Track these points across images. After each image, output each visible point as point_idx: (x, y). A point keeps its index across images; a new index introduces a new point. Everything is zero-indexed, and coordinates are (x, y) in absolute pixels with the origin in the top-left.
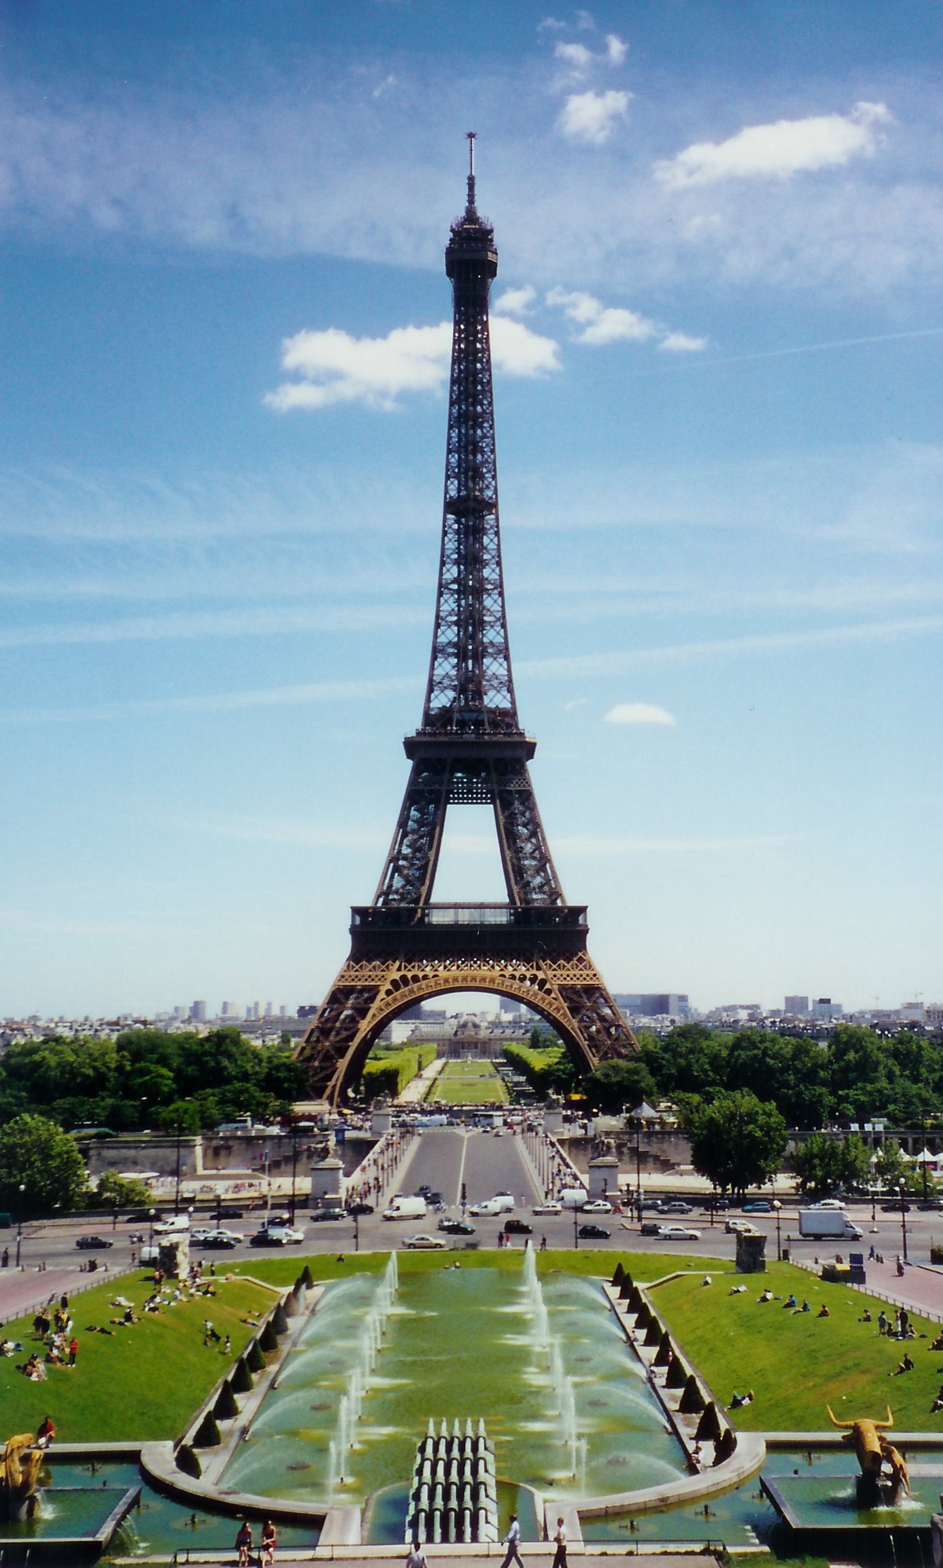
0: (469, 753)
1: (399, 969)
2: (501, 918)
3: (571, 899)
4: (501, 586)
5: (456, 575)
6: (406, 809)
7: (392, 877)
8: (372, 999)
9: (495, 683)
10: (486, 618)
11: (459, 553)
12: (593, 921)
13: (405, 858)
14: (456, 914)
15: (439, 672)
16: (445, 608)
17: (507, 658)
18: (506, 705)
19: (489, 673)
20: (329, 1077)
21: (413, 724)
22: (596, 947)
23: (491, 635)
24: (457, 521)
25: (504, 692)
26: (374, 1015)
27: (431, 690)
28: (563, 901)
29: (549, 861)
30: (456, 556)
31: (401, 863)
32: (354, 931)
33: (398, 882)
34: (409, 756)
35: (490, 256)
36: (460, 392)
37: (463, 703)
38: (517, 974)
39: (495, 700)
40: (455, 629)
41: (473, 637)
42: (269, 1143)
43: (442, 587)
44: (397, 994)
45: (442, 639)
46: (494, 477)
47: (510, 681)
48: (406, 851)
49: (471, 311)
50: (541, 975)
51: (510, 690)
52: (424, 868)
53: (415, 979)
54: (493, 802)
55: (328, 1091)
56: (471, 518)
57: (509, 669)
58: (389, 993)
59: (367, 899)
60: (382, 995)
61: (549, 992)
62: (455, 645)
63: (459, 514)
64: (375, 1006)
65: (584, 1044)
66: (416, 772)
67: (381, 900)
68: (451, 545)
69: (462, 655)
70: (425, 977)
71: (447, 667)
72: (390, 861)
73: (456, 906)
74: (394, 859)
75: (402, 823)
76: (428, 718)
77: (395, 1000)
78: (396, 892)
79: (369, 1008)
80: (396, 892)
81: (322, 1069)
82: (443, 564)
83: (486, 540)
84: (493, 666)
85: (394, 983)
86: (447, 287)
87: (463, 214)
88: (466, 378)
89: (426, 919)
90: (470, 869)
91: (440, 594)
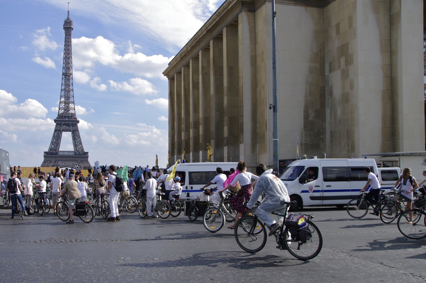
0: (66, 122)
2: (72, 154)
3: (86, 151)
6: (54, 133)
15: (61, 106)
16: (62, 94)
23: (71, 100)
32: (44, 156)
39: (71, 111)
43: (62, 90)
48: (54, 141)
52: (58, 144)
59: (47, 151)
63: (65, 76)
66: (56, 125)
69: (65, 103)
71: (63, 105)
74: (52, 142)
90: (67, 144)
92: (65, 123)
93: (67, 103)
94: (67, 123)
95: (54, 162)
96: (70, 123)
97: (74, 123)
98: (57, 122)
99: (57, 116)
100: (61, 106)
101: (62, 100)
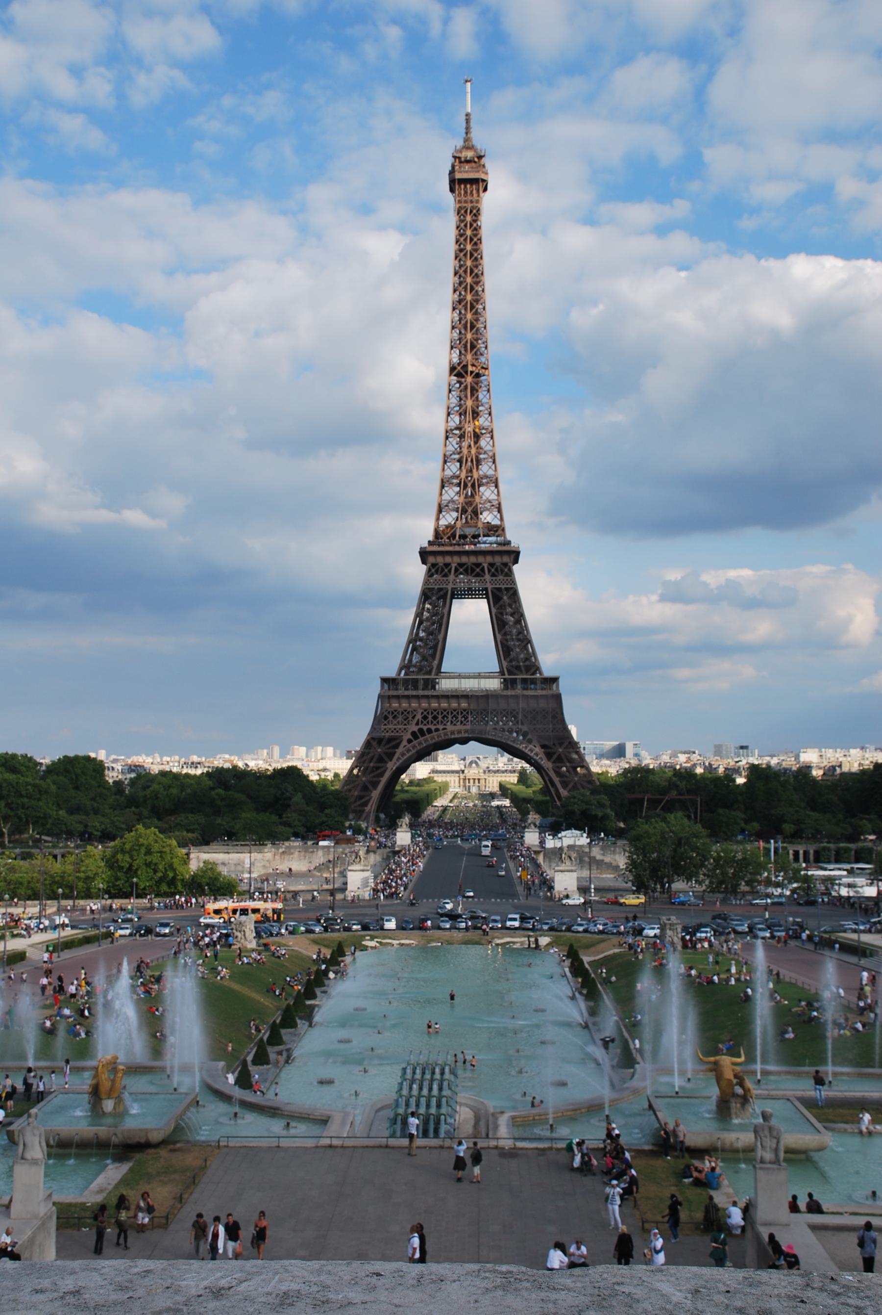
1: (417, 724)
2: (494, 684)
4: (492, 431)
5: (458, 423)
7: (412, 654)
8: (397, 746)
9: (488, 505)
10: (482, 456)
11: (460, 406)
13: (421, 640)
14: (460, 683)
15: (446, 497)
17: (497, 486)
18: (496, 522)
19: (484, 498)
20: (366, 804)
23: (485, 469)
24: (458, 382)
26: (398, 759)
27: (440, 510)
28: (541, 673)
29: (530, 641)
30: (458, 408)
31: (418, 643)
33: (416, 659)
34: (424, 562)
35: (483, 176)
36: (460, 283)
37: (464, 521)
38: (506, 727)
39: (488, 517)
40: (458, 464)
41: (471, 471)
42: (320, 853)
44: (415, 742)
45: (448, 473)
46: (486, 348)
47: (500, 504)
48: (422, 634)
49: (469, 218)
50: (525, 728)
51: (500, 511)
53: (429, 731)
54: (487, 598)
55: (364, 815)
56: (469, 379)
57: (498, 494)
58: (409, 741)
59: (392, 673)
60: (404, 743)
62: (458, 477)
63: (459, 375)
64: (399, 751)
65: (556, 780)
66: (429, 574)
67: (403, 672)
68: (454, 401)
70: (437, 730)
71: (451, 493)
72: (409, 642)
73: (460, 676)
75: (419, 614)
76: (437, 534)
77: (414, 747)
78: (415, 666)
79: (395, 753)
80: (415, 666)
81: (361, 797)
82: (449, 414)
83: (481, 396)
84: (487, 493)
85: (414, 734)
86: (449, 200)
87: (460, 143)
88: (465, 272)
89: (437, 687)
91: (447, 438)
92: (464, 559)
94: (473, 559)
95: (419, 717)
96: (485, 561)
97: (498, 560)
98: (431, 559)
99: (430, 536)
100: (446, 497)
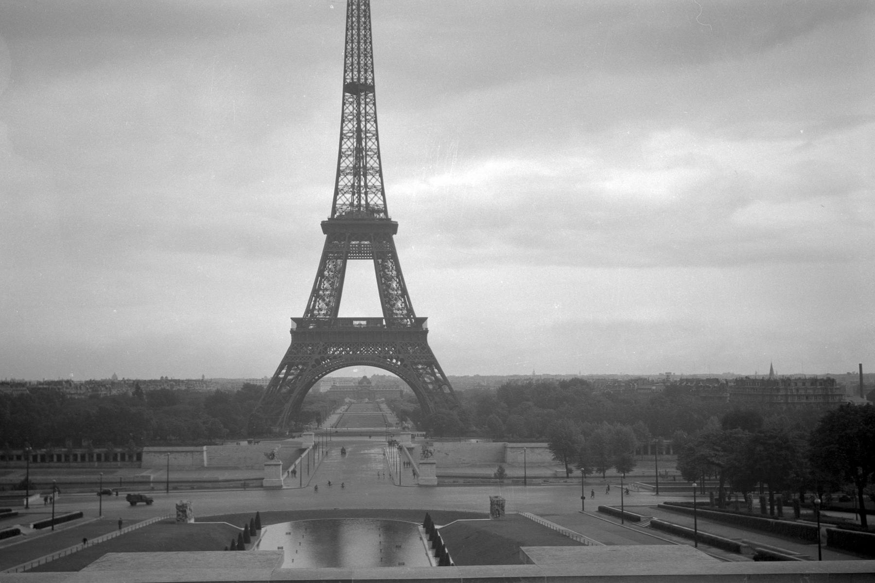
0: (360, 231)
1: (320, 353)
3: (418, 315)
12: (430, 325)
17: (381, 176)
21: (326, 215)
22: (432, 340)
25: (379, 194)
39: (375, 200)
47: (383, 188)
50: (401, 356)
57: (382, 183)
58: (314, 366)
59: (300, 315)
61: (405, 366)
71: (347, 180)
84: (373, 181)
85: (316, 360)
93: (360, 171)
101: (343, 165)
